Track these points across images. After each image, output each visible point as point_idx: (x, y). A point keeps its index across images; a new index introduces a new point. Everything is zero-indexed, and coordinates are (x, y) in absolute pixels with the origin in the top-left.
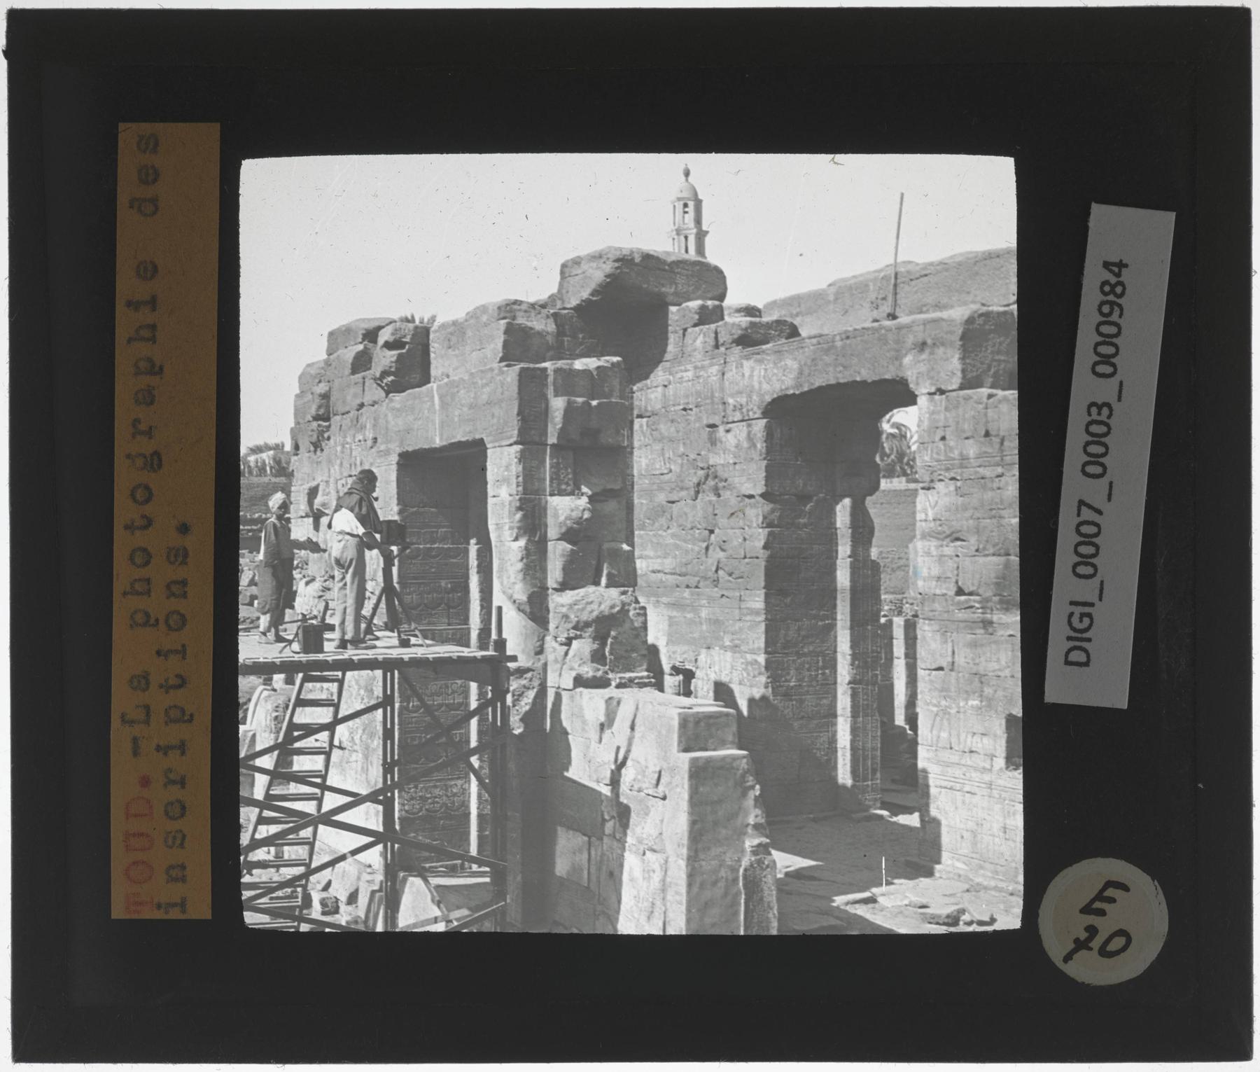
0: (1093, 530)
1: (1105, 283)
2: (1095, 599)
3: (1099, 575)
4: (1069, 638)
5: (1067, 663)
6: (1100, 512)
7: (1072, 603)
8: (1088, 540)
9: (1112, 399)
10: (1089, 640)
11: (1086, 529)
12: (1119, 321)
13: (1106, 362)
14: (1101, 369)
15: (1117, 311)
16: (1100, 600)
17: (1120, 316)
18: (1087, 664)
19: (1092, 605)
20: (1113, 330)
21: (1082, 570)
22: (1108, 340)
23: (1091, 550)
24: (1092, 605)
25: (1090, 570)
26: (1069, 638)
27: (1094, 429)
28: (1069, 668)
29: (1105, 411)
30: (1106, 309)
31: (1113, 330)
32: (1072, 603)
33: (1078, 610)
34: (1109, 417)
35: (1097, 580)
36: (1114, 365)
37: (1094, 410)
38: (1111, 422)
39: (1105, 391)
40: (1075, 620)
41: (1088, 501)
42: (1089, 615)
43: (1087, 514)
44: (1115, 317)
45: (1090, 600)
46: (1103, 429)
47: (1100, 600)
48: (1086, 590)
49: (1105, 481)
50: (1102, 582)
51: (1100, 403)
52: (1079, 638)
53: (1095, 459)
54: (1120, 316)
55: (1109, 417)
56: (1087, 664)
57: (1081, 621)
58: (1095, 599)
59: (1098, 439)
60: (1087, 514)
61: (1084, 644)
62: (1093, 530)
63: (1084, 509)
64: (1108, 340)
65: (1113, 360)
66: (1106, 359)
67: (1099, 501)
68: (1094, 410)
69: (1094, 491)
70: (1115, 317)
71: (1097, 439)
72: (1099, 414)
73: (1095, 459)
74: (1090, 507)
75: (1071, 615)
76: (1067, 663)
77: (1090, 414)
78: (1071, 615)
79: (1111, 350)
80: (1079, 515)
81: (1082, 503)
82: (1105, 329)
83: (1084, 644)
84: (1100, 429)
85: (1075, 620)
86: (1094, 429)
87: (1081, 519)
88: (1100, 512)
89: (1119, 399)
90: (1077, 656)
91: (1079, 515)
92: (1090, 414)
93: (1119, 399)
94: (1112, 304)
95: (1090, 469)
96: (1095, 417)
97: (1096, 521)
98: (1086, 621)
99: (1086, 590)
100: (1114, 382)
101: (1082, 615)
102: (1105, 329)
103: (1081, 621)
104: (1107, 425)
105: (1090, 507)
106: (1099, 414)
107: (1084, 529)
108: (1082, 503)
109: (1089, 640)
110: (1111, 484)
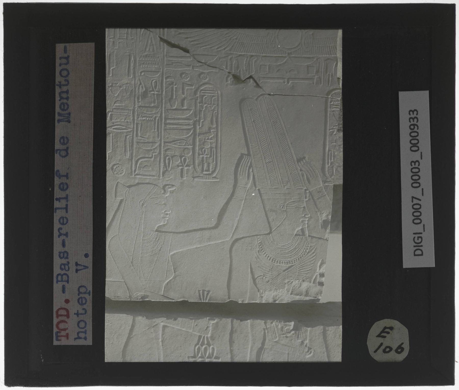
0: (418, 207)
1: (410, 118)
2: (421, 231)
3: (422, 222)
4: (414, 246)
5: (415, 255)
6: (420, 200)
7: (414, 234)
8: (417, 210)
9: (419, 159)
10: (422, 246)
11: (415, 207)
12: (417, 131)
13: (415, 146)
14: (414, 149)
15: (416, 127)
16: (424, 231)
17: (418, 129)
18: (422, 255)
19: (421, 233)
20: (416, 134)
21: (416, 221)
22: (414, 138)
23: (419, 214)
24: (421, 233)
25: (419, 221)
26: (414, 246)
27: (414, 170)
28: (416, 256)
29: (417, 163)
30: (412, 127)
31: (416, 134)
32: (414, 234)
33: (416, 236)
34: (419, 165)
35: (422, 225)
36: (418, 147)
37: (413, 164)
38: (419, 167)
39: (416, 156)
40: (416, 239)
41: (415, 196)
42: (421, 237)
43: (415, 201)
44: (416, 130)
45: (420, 232)
46: (417, 170)
47: (424, 231)
48: (419, 229)
49: (420, 189)
50: (424, 225)
51: (415, 161)
52: (418, 246)
53: (416, 181)
54: (418, 129)
55: (419, 165)
56: (422, 255)
57: (418, 239)
58: (421, 231)
59: (416, 174)
60: (415, 201)
61: (420, 248)
62: (418, 207)
63: (414, 199)
64: (414, 138)
65: (417, 145)
66: (415, 145)
67: (419, 196)
68: (413, 164)
69: (417, 193)
70: (416, 130)
71: (415, 174)
72: (415, 165)
73: (416, 181)
74: (416, 198)
75: (414, 238)
76: (415, 255)
77: (412, 165)
78: (414, 238)
79: (416, 142)
80: (412, 202)
81: (413, 197)
82: (413, 134)
83: (420, 248)
84: (417, 170)
85: (416, 239)
86: (414, 170)
87: (413, 203)
88: (420, 200)
89: (421, 159)
90: (419, 252)
91: (412, 202)
92: (412, 165)
93: (421, 159)
94: (414, 125)
95: (415, 185)
96: (414, 166)
97: (419, 203)
98: (420, 239)
99: (419, 229)
100: (419, 153)
101: (418, 237)
102: (413, 134)
103: (418, 239)
104: (419, 169)
105: (416, 198)
106: (415, 165)
107: (415, 207)
108: (413, 197)
109: (422, 246)
110: (423, 189)
